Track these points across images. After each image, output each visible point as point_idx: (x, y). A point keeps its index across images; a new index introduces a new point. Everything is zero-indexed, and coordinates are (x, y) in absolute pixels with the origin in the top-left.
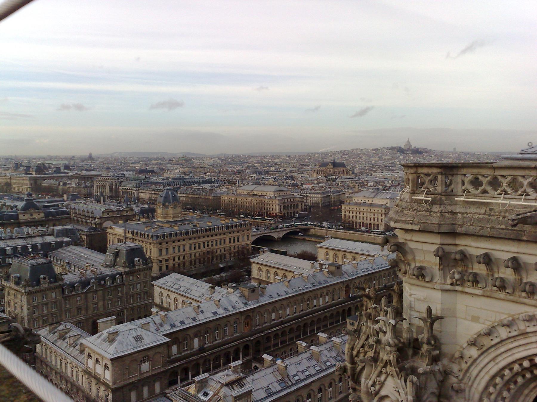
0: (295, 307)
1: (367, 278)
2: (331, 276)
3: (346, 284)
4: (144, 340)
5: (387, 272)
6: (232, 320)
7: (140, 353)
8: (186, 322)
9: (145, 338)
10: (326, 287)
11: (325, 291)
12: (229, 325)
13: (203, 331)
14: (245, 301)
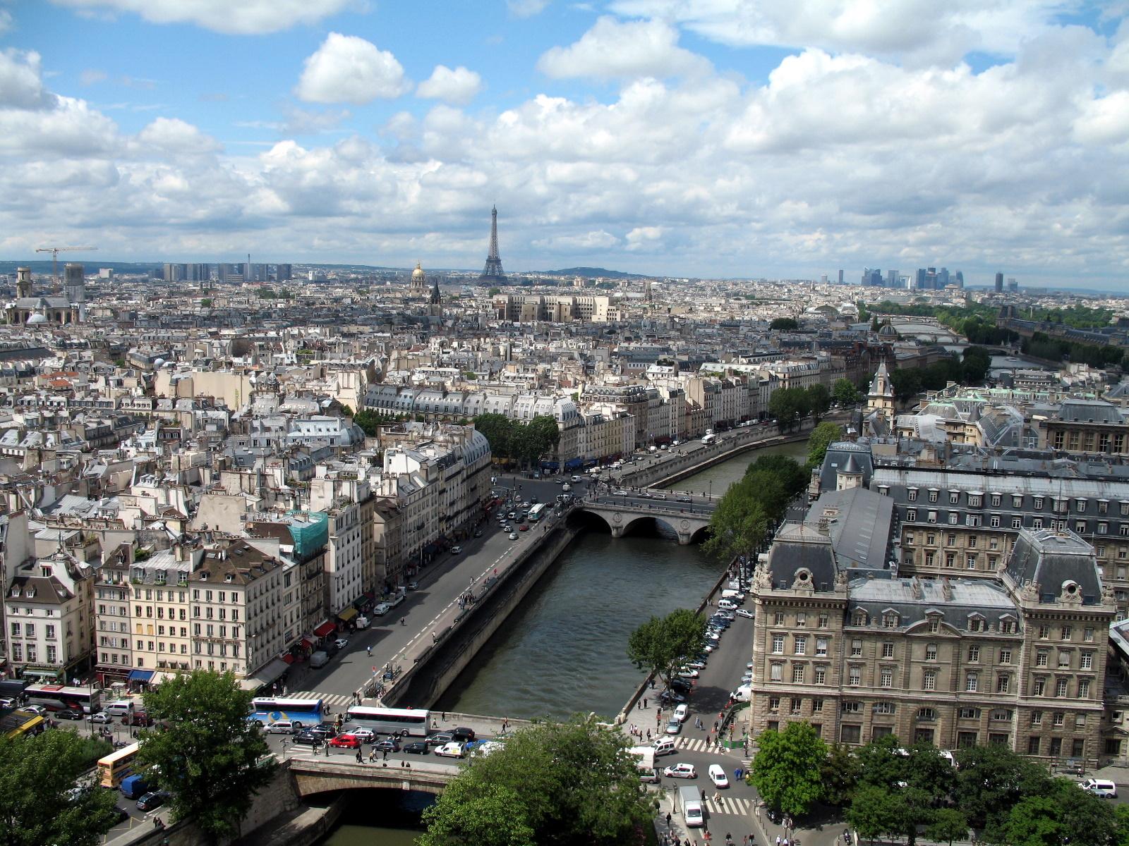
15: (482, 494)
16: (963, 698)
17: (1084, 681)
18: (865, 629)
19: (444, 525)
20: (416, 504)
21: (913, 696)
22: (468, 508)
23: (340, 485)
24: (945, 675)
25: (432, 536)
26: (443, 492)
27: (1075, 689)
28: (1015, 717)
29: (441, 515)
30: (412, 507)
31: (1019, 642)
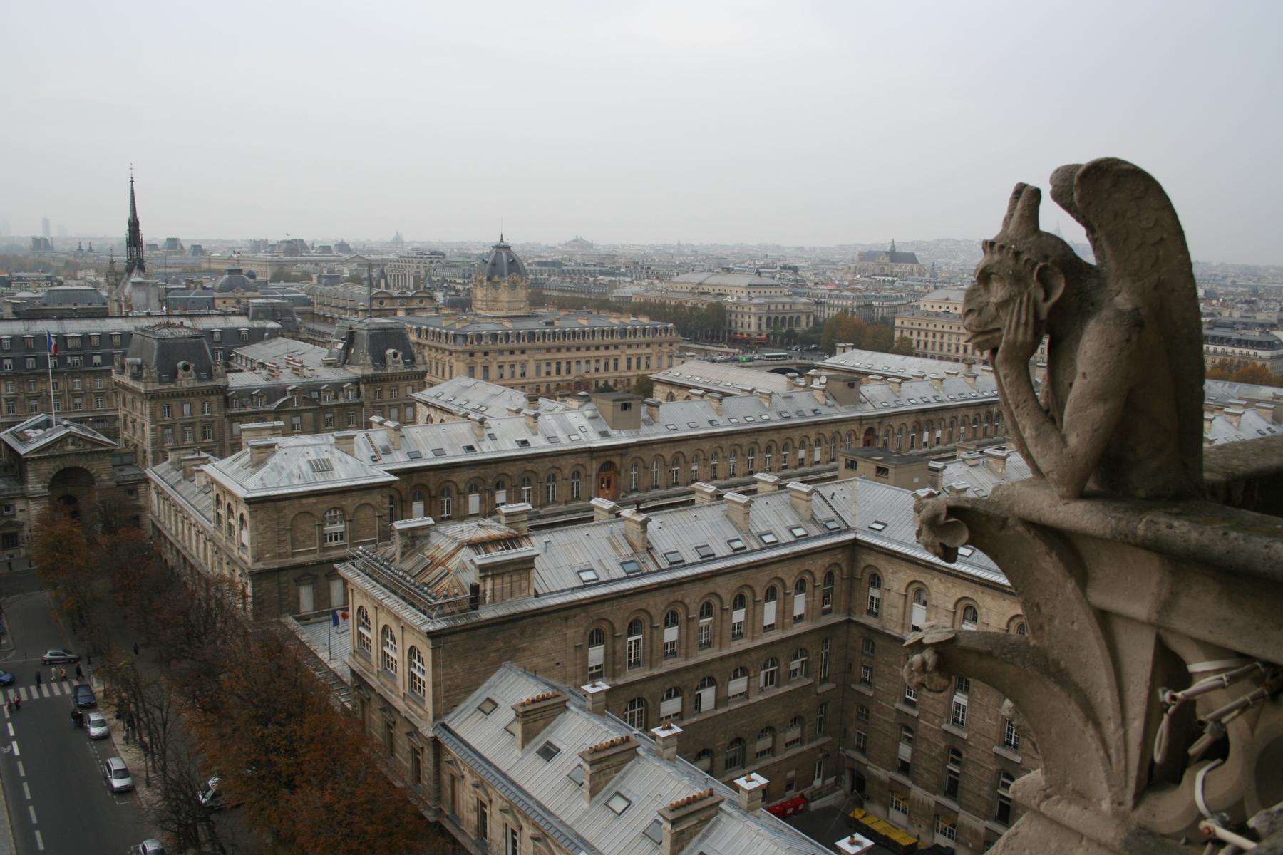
0: (733, 461)
1: (923, 418)
2: (830, 402)
3: (866, 427)
4: (335, 472)
5: (971, 413)
6: (567, 465)
7: (321, 499)
8: (449, 453)
9: (337, 467)
10: (816, 424)
11: (812, 434)
12: (559, 477)
13: (490, 481)
14: (608, 429)
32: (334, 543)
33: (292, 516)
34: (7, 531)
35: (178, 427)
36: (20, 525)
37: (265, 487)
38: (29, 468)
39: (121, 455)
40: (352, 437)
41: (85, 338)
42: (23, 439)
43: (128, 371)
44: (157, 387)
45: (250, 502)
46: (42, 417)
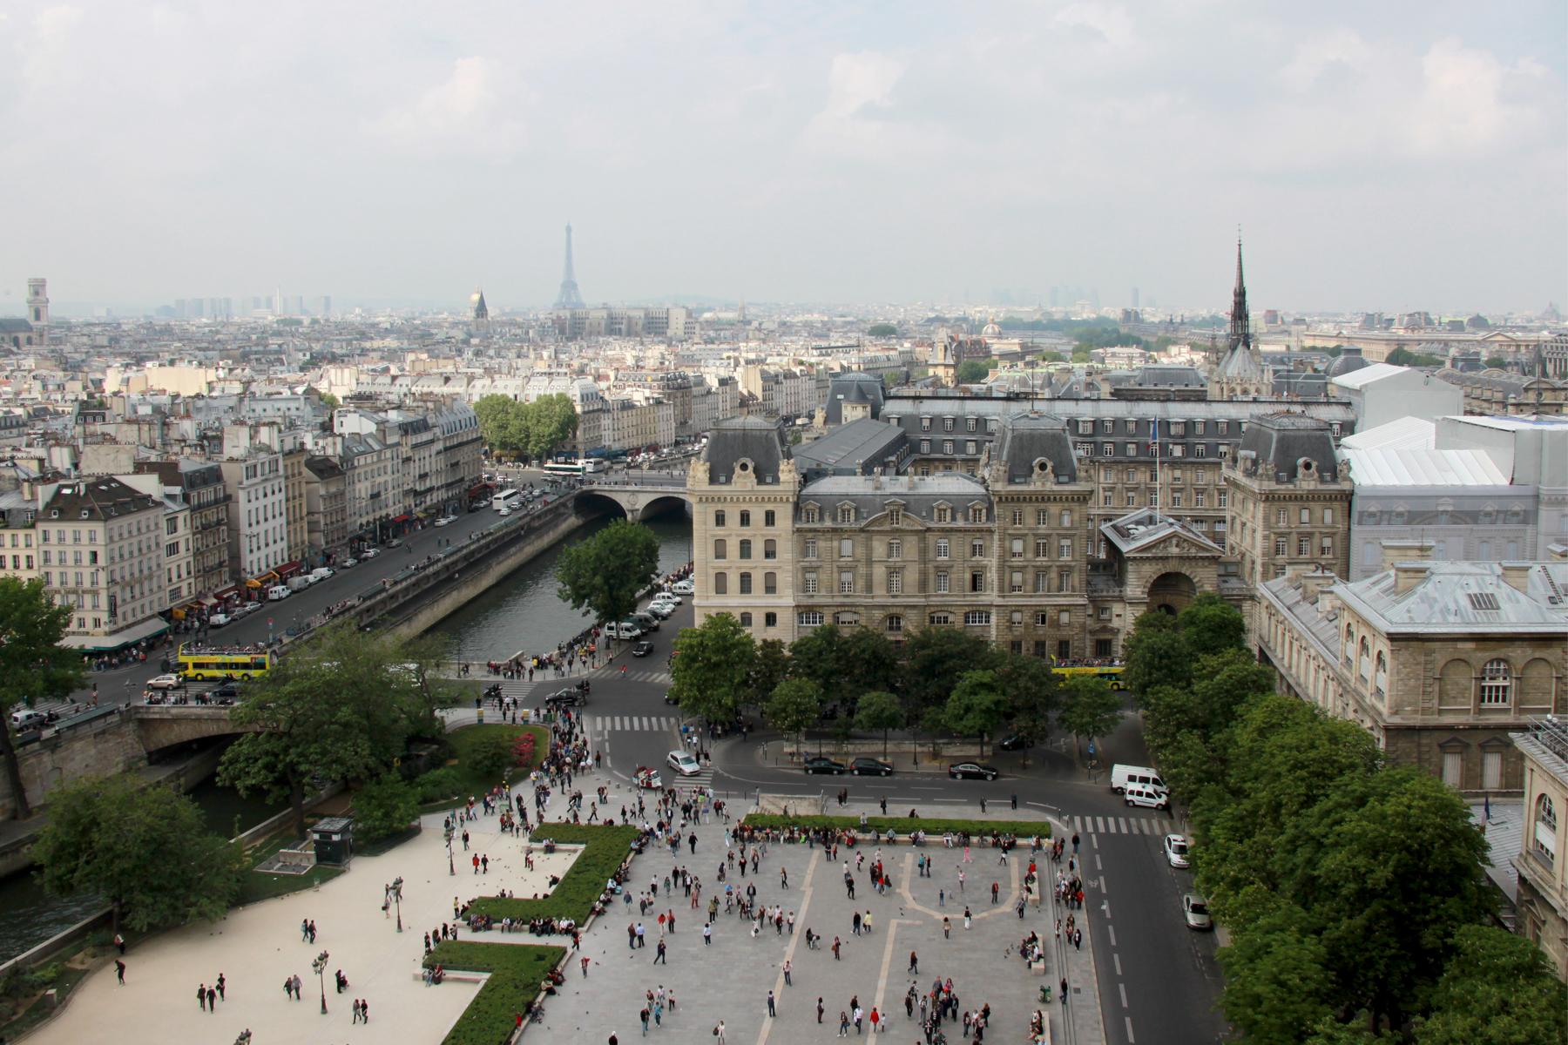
15: (466, 473)
16: (934, 600)
17: (1064, 571)
18: (817, 525)
19: (411, 501)
20: (369, 469)
21: (877, 601)
22: (448, 486)
23: (257, 432)
24: (912, 575)
25: (394, 511)
26: (408, 459)
27: (1055, 583)
28: (993, 619)
29: (406, 487)
30: (362, 471)
31: (990, 531)
32: (1493, 705)
33: (1442, 663)
34: (1103, 637)
35: (1294, 537)
36: (1116, 632)
37: (1412, 621)
38: (1130, 567)
39: (1226, 564)
40: (1527, 569)
41: (1189, 425)
42: (1124, 533)
43: (1240, 464)
44: (1273, 486)
45: (1393, 638)
46: (1145, 512)
